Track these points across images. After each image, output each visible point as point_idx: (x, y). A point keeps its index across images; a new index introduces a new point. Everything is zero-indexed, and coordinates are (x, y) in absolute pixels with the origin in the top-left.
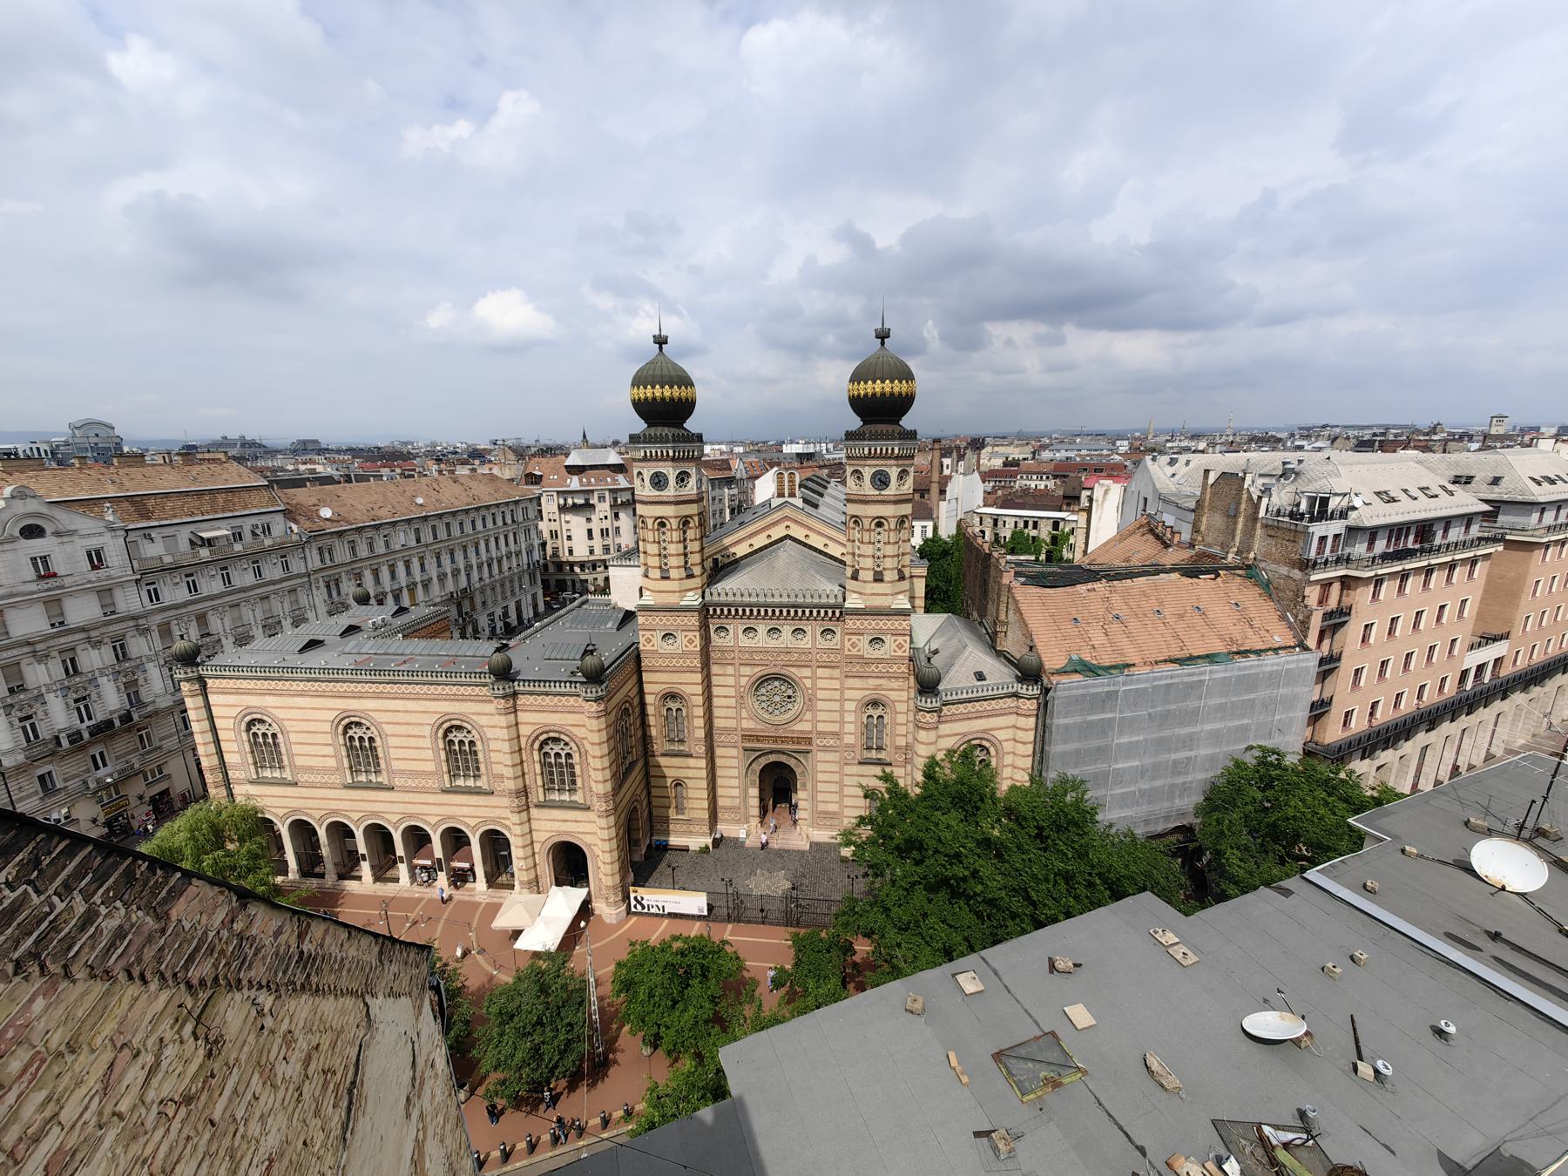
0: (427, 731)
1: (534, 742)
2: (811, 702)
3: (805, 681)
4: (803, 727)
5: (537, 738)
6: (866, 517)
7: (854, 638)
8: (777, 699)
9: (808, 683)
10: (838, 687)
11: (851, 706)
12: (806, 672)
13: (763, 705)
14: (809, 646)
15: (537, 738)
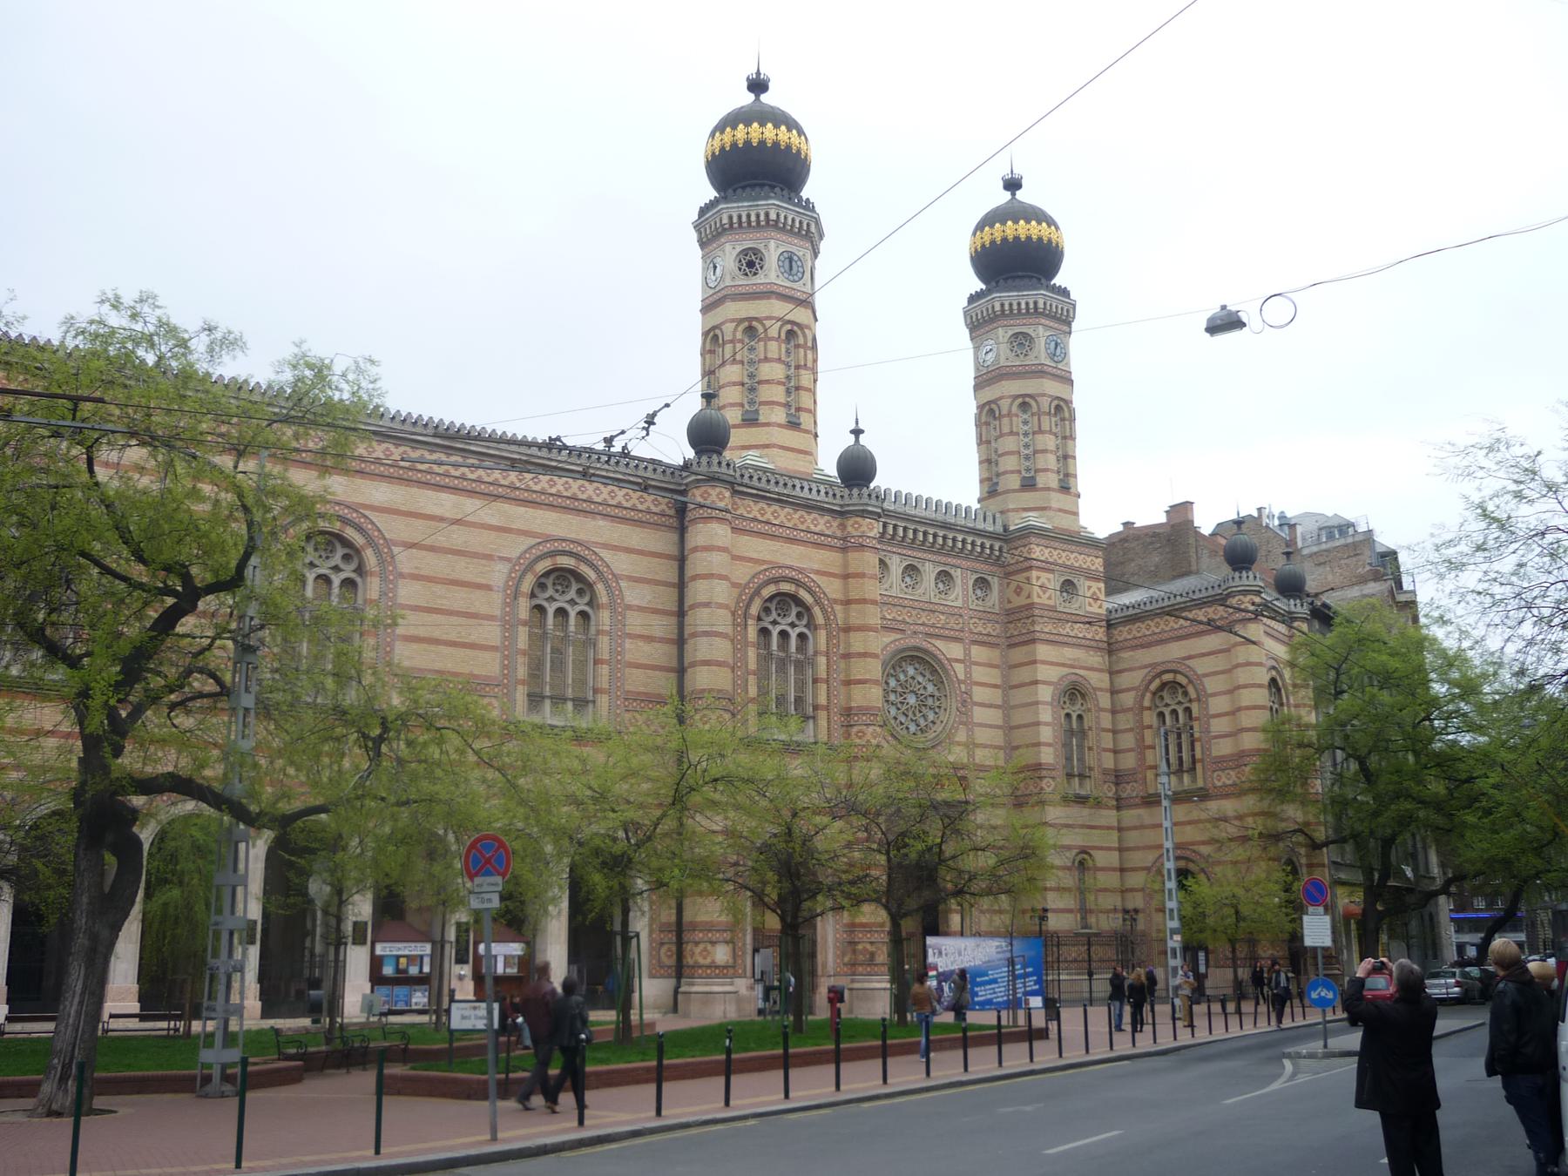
0: (498, 574)
1: (751, 600)
2: (966, 703)
3: (956, 666)
4: (957, 755)
5: (757, 592)
6: (1044, 395)
7: (1044, 576)
8: (912, 700)
9: (959, 668)
10: (999, 682)
11: (1045, 693)
12: (953, 650)
13: (893, 711)
14: (959, 603)
15: (757, 592)
